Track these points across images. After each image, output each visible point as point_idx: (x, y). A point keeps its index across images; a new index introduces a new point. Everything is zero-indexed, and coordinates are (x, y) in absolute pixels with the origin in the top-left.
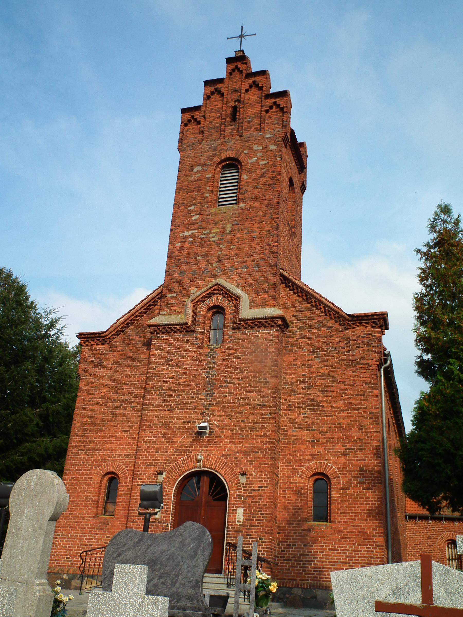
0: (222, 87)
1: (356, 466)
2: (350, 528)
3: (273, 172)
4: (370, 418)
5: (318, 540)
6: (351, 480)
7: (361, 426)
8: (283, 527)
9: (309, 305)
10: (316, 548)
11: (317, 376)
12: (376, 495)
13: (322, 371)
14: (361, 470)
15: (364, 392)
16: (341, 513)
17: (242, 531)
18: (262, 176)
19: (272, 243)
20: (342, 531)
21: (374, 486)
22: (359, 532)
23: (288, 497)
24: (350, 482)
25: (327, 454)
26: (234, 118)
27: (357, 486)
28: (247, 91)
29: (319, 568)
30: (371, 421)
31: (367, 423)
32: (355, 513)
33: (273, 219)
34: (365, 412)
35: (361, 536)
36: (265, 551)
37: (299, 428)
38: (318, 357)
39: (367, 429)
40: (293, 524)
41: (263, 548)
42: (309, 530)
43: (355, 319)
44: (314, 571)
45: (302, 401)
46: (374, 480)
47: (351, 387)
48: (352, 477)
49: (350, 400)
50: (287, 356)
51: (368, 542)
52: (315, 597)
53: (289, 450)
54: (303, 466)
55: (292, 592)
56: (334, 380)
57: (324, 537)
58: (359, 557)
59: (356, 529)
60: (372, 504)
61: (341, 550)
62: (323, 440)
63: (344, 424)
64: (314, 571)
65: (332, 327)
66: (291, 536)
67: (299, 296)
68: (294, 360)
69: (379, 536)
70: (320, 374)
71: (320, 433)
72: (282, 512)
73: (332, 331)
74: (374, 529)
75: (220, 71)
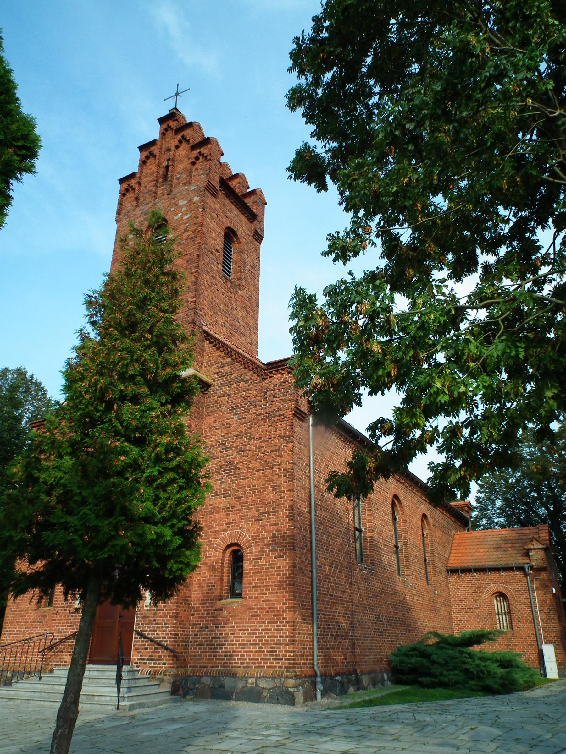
0: (155, 150)
1: (269, 532)
2: (261, 604)
3: (195, 224)
4: (284, 476)
5: (229, 620)
6: (263, 548)
7: (275, 486)
8: (197, 607)
9: (229, 360)
10: (227, 630)
11: (235, 436)
12: (287, 563)
13: (239, 430)
14: (274, 536)
15: (279, 447)
16: (253, 587)
17: (148, 617)
18: (186, 230)
19: (190, 300)
20: (253, 609)
21: (286, 553)
22: (269, 608)
23: (203, 574)
24: (262, 552)
25: (241, 522)
26: (165, 177)
27: (269, 554)
28: (177, 147)
29: (229, 652)
30: (284, 479)
31: (281, 482)
32: (266, 586)
33: (192, 273)
34: (280, 470)
35: (272, 612)
36: (168, 638)
37: (216, 495)
38: (236, 414)
39: (281, 488)
40: (206, 603)
41: (167, 634)
42: (221, 610)
43: (270, 367)
44: (225, 656)
45: (220, 466)
46: (286, 546)
47: (267, 443)
48: (265, 545)
49: (266, 458)
50: (208, 417)
51: (278, 619)
52: (222, 686)
53: (206, 521)
54: (218, 538)
55: (202, 681)
56: (251, 438)
57: (235, 616)
58: (268, 637)
59: (266, 605)
60: (283, 574)
61: (251, 630)
62: (238, 507)
63: (259, 486)
64: (225, 656)
65: (250, 379)
66: (204, 617)
67: (221, 351)
68: (215, 422)
69: (289, 611)
70: (238, 433)
71: (235, 498)
72: (196, 591)
73: (251, 384)
74: (284, 604)
75: (153, 132)
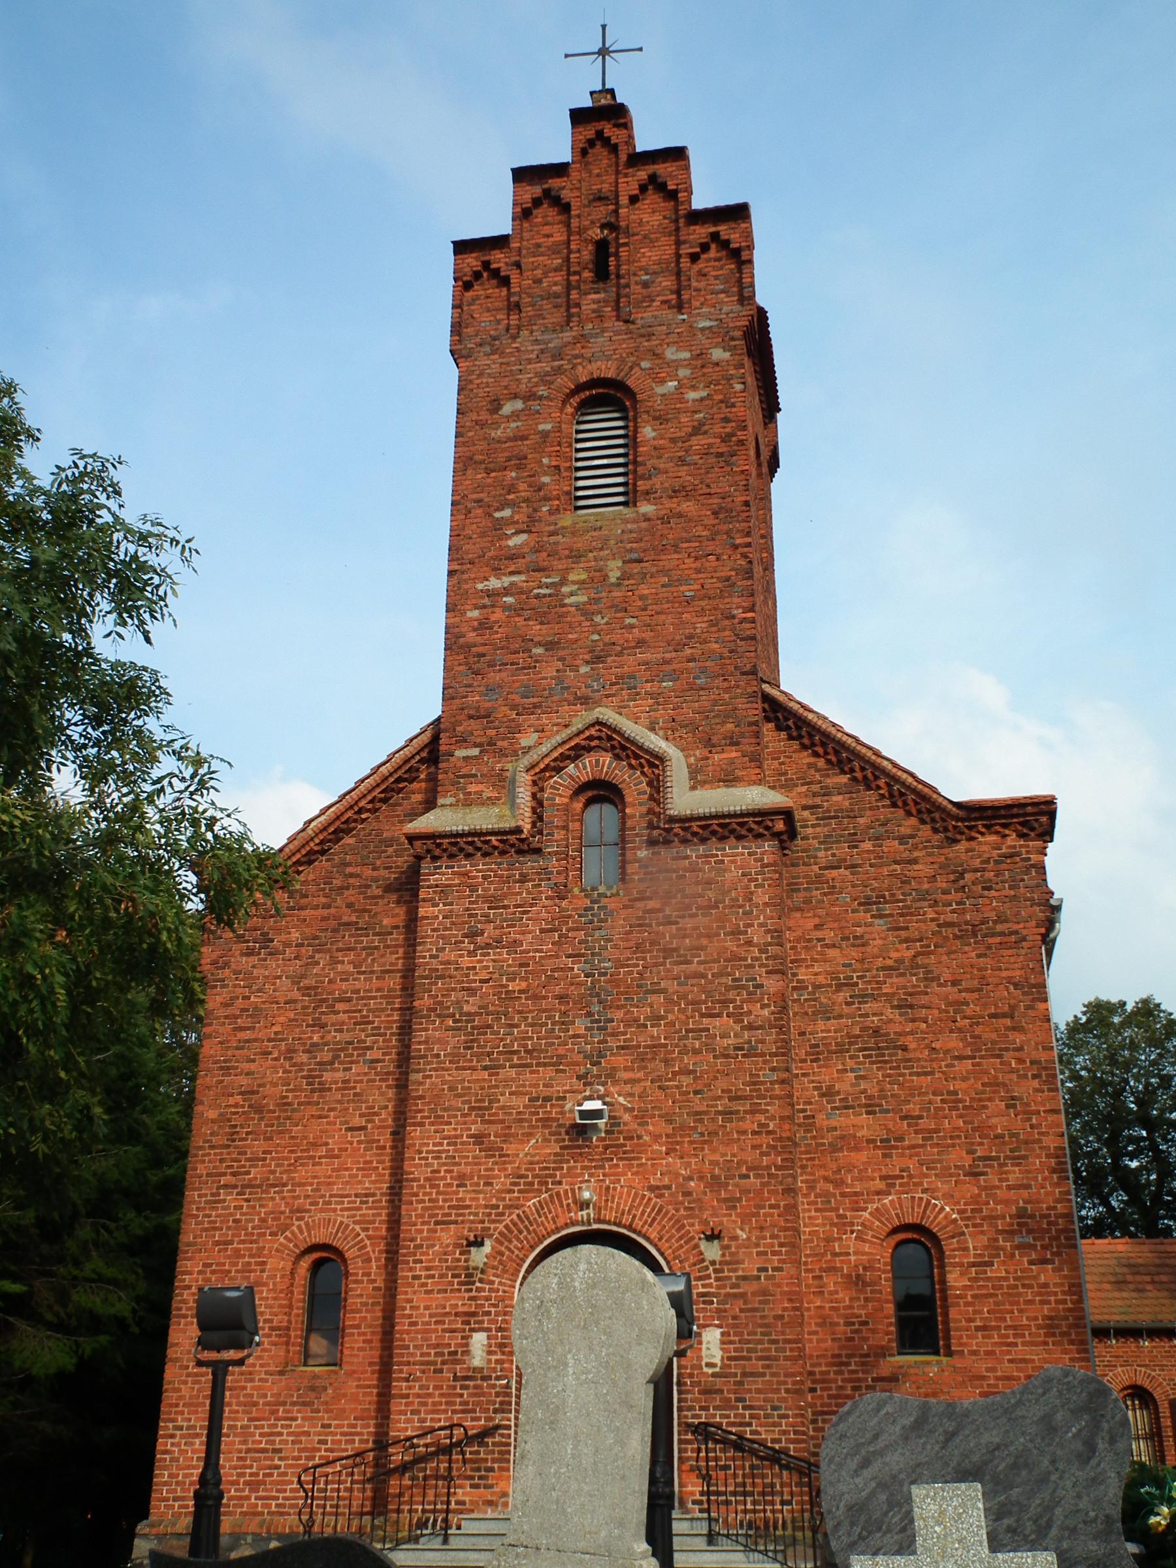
0: (565, 188)
1: (1006, 1202)
2: (1005, 1368)
3: (726, 420)
4: (1034, 1077)
6: (996, 1240)
7: (1013, 1098)
8: (822, 1373)
9: (844, 779)
11: (883, 968)
12: (1065, 1277)
13: (894, 955)
14: (1021, 1214)
15: (1013, 1008)
16: (978, 1329)
18: (697, 430)
20: (984, 1378)
21: (1058, 1254)
23: (831, 1293)
24: (993, 1247)
25: (926, 1176)
26: (601, 272)
27: (1013, 1255)
30: (1036, 1083)
31: (1027, 1089)
32: (1014, 1328)
33: (736, 547)
34: (1020, 1061)
37: (846, 1108)
38: (881, 916)
39: (1028, 1105)
40: (848, 1364)
41: (784, 1432)
45: (849, 1036)
46: (1057, 1238)
47: (976, 995)
48: (999, 1232)
49: (978, 1030)
50: (798, 915)
54: (865, 1209)
59: (1019, 1370)
60: (1057, 1302)
63: (965, 1092)
65: (912, 836)
67: (816, 754)
68: (817, 927)
70: (890, 962)
71: (903, 1118)
73: (915, 847)
75: (557, 146)
